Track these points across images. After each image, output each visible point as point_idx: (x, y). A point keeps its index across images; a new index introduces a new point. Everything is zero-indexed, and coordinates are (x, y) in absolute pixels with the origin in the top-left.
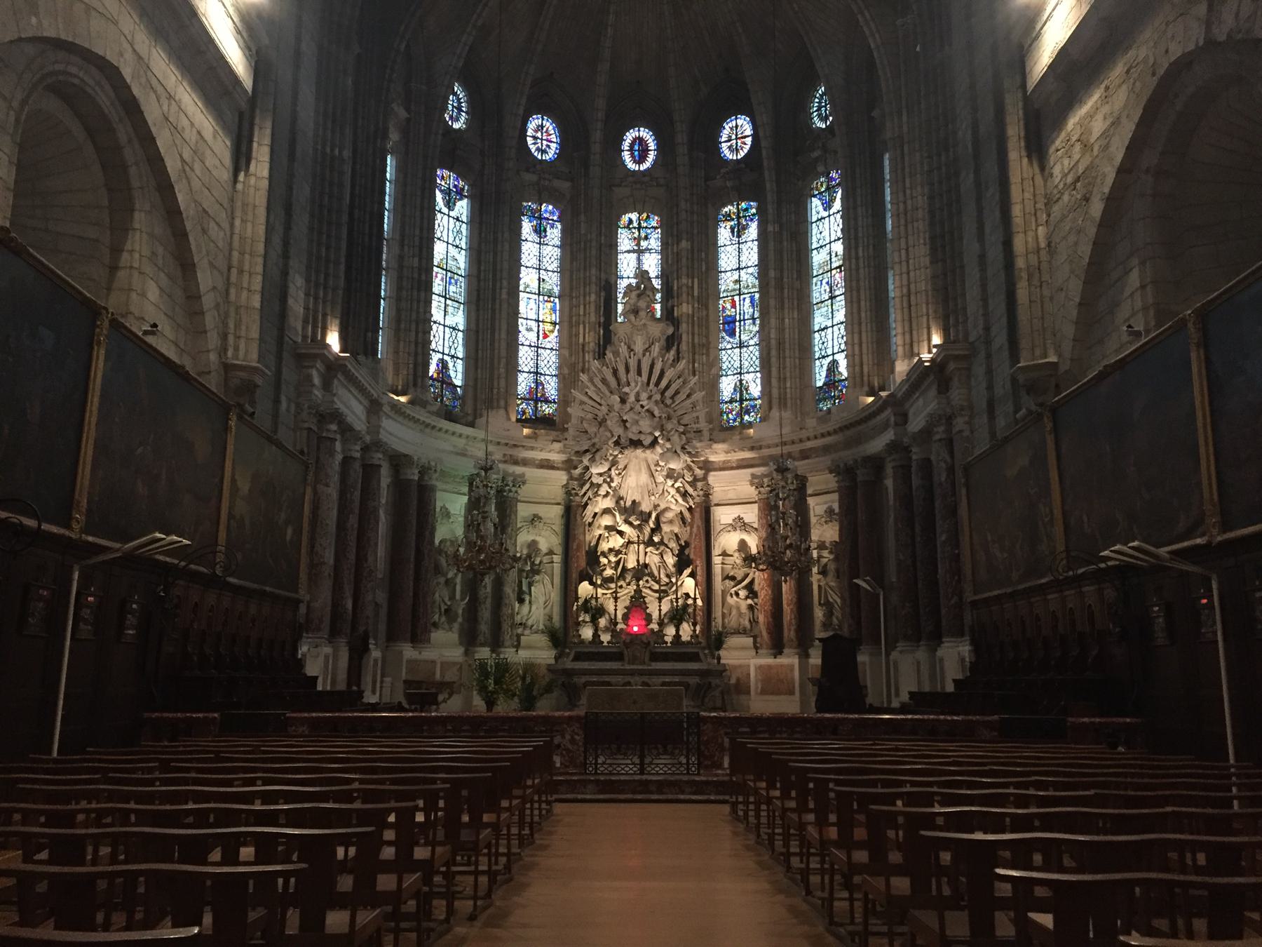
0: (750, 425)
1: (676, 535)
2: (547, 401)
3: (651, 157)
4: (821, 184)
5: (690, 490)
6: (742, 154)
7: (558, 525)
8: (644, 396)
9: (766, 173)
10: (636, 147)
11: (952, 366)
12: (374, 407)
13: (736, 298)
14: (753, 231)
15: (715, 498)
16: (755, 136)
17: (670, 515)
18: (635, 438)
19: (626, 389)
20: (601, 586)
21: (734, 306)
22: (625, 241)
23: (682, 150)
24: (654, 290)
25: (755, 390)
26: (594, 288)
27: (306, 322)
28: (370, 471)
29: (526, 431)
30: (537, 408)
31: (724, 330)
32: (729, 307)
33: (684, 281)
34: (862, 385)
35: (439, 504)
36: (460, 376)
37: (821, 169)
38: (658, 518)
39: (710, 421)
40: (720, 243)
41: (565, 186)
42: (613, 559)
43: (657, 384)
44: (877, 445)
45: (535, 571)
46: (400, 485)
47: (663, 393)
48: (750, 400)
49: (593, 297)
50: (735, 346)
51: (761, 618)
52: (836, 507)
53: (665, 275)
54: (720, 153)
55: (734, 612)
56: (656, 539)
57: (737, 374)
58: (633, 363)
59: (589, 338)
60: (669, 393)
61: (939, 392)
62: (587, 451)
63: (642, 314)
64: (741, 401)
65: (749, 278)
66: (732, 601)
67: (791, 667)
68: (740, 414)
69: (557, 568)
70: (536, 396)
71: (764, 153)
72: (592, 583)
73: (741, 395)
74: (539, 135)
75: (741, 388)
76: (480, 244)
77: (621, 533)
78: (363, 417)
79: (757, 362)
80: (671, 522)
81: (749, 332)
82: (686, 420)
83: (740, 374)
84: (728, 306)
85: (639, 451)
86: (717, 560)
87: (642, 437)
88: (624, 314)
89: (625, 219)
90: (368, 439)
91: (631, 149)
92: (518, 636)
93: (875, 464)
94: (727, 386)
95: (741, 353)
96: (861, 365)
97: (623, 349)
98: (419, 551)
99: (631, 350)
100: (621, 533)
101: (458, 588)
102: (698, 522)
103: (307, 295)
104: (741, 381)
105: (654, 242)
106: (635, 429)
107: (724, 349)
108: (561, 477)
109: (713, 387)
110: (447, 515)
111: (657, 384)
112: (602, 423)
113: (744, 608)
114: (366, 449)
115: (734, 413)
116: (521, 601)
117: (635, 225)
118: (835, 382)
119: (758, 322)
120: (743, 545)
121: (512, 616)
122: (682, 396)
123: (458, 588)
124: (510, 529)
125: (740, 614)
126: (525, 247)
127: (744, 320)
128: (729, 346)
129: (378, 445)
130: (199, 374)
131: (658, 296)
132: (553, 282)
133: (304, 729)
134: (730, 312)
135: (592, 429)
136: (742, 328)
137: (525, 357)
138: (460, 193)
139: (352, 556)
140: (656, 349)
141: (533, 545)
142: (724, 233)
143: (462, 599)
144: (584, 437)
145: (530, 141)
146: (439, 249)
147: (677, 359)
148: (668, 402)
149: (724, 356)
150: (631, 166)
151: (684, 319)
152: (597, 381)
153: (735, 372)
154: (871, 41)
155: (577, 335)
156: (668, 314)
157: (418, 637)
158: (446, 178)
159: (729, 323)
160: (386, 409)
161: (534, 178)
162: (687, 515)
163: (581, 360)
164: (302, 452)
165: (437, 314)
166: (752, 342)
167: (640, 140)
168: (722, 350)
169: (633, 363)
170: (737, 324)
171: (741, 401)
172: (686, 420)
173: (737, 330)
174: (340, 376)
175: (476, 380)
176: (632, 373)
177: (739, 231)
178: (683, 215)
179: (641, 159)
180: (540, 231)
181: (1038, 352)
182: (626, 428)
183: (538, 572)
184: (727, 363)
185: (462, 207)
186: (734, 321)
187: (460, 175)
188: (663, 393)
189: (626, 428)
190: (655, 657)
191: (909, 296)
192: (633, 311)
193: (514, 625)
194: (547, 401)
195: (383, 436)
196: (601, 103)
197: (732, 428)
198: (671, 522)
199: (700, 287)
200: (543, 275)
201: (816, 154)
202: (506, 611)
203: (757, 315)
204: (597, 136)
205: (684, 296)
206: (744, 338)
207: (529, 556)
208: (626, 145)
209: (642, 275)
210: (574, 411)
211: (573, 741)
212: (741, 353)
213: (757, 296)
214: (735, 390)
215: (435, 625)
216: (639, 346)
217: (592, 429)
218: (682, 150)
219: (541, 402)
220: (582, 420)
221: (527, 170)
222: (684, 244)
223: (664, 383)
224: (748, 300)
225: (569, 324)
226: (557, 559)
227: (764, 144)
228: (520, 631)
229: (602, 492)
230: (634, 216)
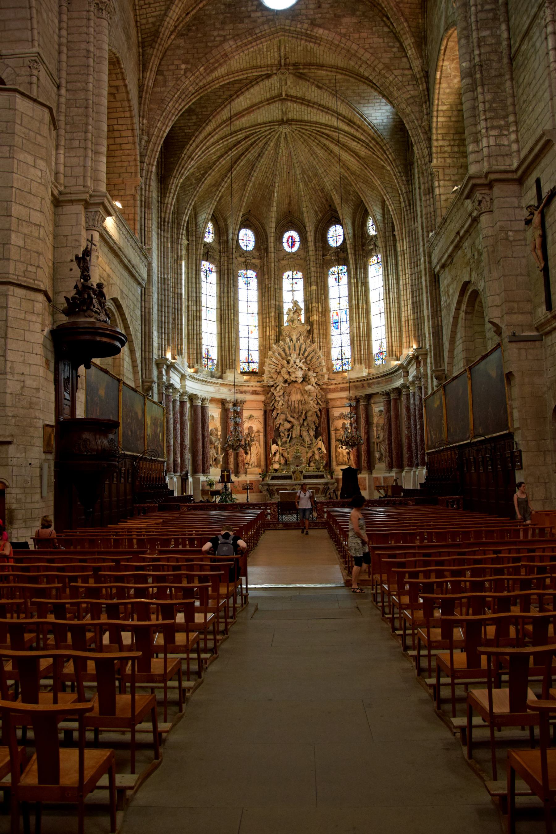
0: (346, 371)
2: (254, 363)
3: (297, 245)
4: (373, 260)
5: (320, 402)
6: (339, 244)
7: (262, 420)
8: (298, 361)
9: (350, 256)
10: (290, 240)
11: (420, 358)
12: (183, 377)
13: (338, 311)
14: (345, 279)
15: (331, 404)
16: (344, 235)
17: (309, 414)
18: (294, 380)
19: (289, 358)
20: (281, 446)
21: (337, 315)
22: (286, 284)
23: (311, 244)
24: (300, 309)
26: (273, 310)
27: (159, 349)
28: (182, 403)
29: (245, 378)
33: (315, 305)
34: (392, 356)
35: (210, 414)
37: (374, 254)
38: (306, 413)
39: (328, 370)
40: (330, 285)
41: (257, 262)
42: (286, 433)
43: (303, 355)
44: (399, 383)
45: (252, 440)
46: (193, 407)
47: (306, 358)
49: (273, 314)
51: (352, 458)
52: (382, 408)
53: (307, 302)
54: (328, 244)
55: (341, 455)
56: (305, 424)
58: (292, 346)
59: (272, 334)
60: (308, 359)
61: (417, 367)
62: (273, 386)
63: (296, 322)
64: (342, 359)
65: (345, 304)
66: (340, 450)
67: (365, 478)
69: (262, 438)
71: (348, 246)
72: (277, 445)
74: (244, 238)
76: (220, 293)
77: (289, 422)
78: (179, 382)
79: (349, 342)
81: (345, 327)
82: (317, 370)
84: (335, 314)
85: (296, 385)
86: (332, 432)
87: (297, 380)
88: (287, 322)
89: (285, 275)
90: (182, 392)
91: (288, 242)
92: (246, 469)
93: (398, 391)
94: (335, 354)
96: (392, 347)
97: (288, 340)
98: (203, 436)
99: (291, 340)
100: (289, 422)
101: (219, 449)
102: (324, 416)
103: (159, 338)
105: (300, 284)
106: (293, 376)
108: (262, 398)
109: (328, 354)
110: (213, 417)
111: (303, 355)
112: (279, 373)
113: (345, 454)
114: (181, 395)
116: (246, 453)
117: (291, 277)
120: (344, 424)
121: (243, 461)
122: (314, 360)
123: (219, 449)
125: (343, 456)
126: (240, 291)
129: (185, 393)
130: (137, 387)
131: (303, 312)
132: (255, 308)
133: (186, 509)
135: (275, 376)
137: (243, 344)
138: (211, 271)
139: (179, 441)
140: (302, 339)
141: (250, 428)
142: (331, 280)
143: (221, 454)
144: (271, 380)
145: (240, 242)
146: (204, 298)
147: (312, 342)
148: (308, 362)
149: (333, 338)
150: (288, 250)
151: (315, 322)
152: (276, 354)
154: (389, 207)
155: (266, 331)
156: (308, 319)
157: (205, 472)
158: (206, 265)
160: (188, 377)
161: (243, 259)
162: (319, 413)
164: (161, 403)
165: (204, 328)
167: (292, 237)
169: (292, 346)
171: (342, 359)
172: (317, 370)
174: (172, 369)
175: (222, 356)
176: (291, 350)
177: (338, 280)
178: (313, 274)
179: (293, 246)
180: (247, 283)
181: (439, 365)
182: (290, 375)
183: (253, 441)
185: (213, 277)
187: (212, 263)
188: (306, 358)
189: (290, 375)
190: (305, 477)
191: (408, 321)
192: (291, 321)
193: (244, 464)
195: (187, 389)
196: (273, 225)
197: (338, 372)
198: (312, 416)
199: (322, 307)
200: (249, 304)
201: (371, 247)
202: (240, 458)
203: (348, 319)
204: (272, 239)
205: (315, 312)
206: (343, 331)
207: (249, 434)
208: (285, 240)
209: (295, 303)
210: (266, 368)
211: (274, 511)
215: (211, 465)
216: (295, 337)
217: (275, 376)
218: (311, 244)
220: (270, 372)
221: (240, 256)
222: (314, 287)
223: (306, 354)
224: (344, 312)
225: (263, 325)
226: (262, 434)
227: (348, 242)
228: (247, 466)
229: (280, 404)
230: (290, 273)
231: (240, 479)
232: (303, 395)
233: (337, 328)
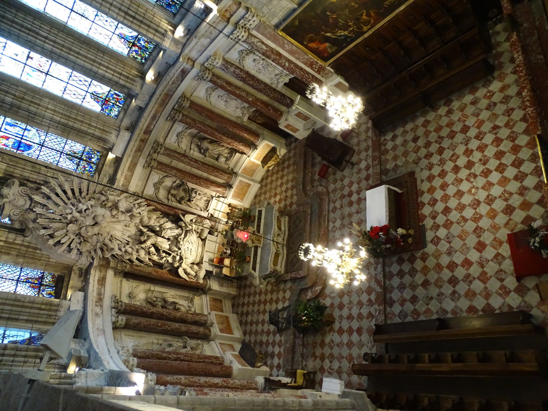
1: (157, 218)
2: (42, 278)
17: (146, 219)
21: (8, 138)
25: (78, 147)
30: (46, 286)
31: (23, 151)
32: (7, 142)
36: (21, 333)
43: (69, 199)
48: (83, 153)
50: (40, 148)
57: (61, 155)
68: (89, 163)
70: (38, 284)
73: (77, 157)
75: (72, 156)
80: (150, 218)
83: (62, 153)
94: (67, 164)
95: (47, 147)
104: (67, 154)
107: (38, 156)
115: (86, 166)
118: (105, 99)
119: (29, 127)
124: (144, 309)
127: (23, 136)
128: (38, 152)
134: (10, 142)
136: (28, 139)
153: (59, 155)
159: (19, 146)
163: (18, 247)
166: (43, 137)
168: (37, 158)
170: (23, 141)
171: (81, 159)
173: (28, 143)
175: (27, 321)
184: (49, 158)
186: (20, 142)
194: (42, 278)
198: (150, 218)
203: (24, 126)
206: (37, 141)
212: (47, 147)
213: (8, 120)
214: (71, 160)
219: (42, 281)
224: (8, 127)
231: (215, 321)
232: (119, 222)
233: (29, 147)
